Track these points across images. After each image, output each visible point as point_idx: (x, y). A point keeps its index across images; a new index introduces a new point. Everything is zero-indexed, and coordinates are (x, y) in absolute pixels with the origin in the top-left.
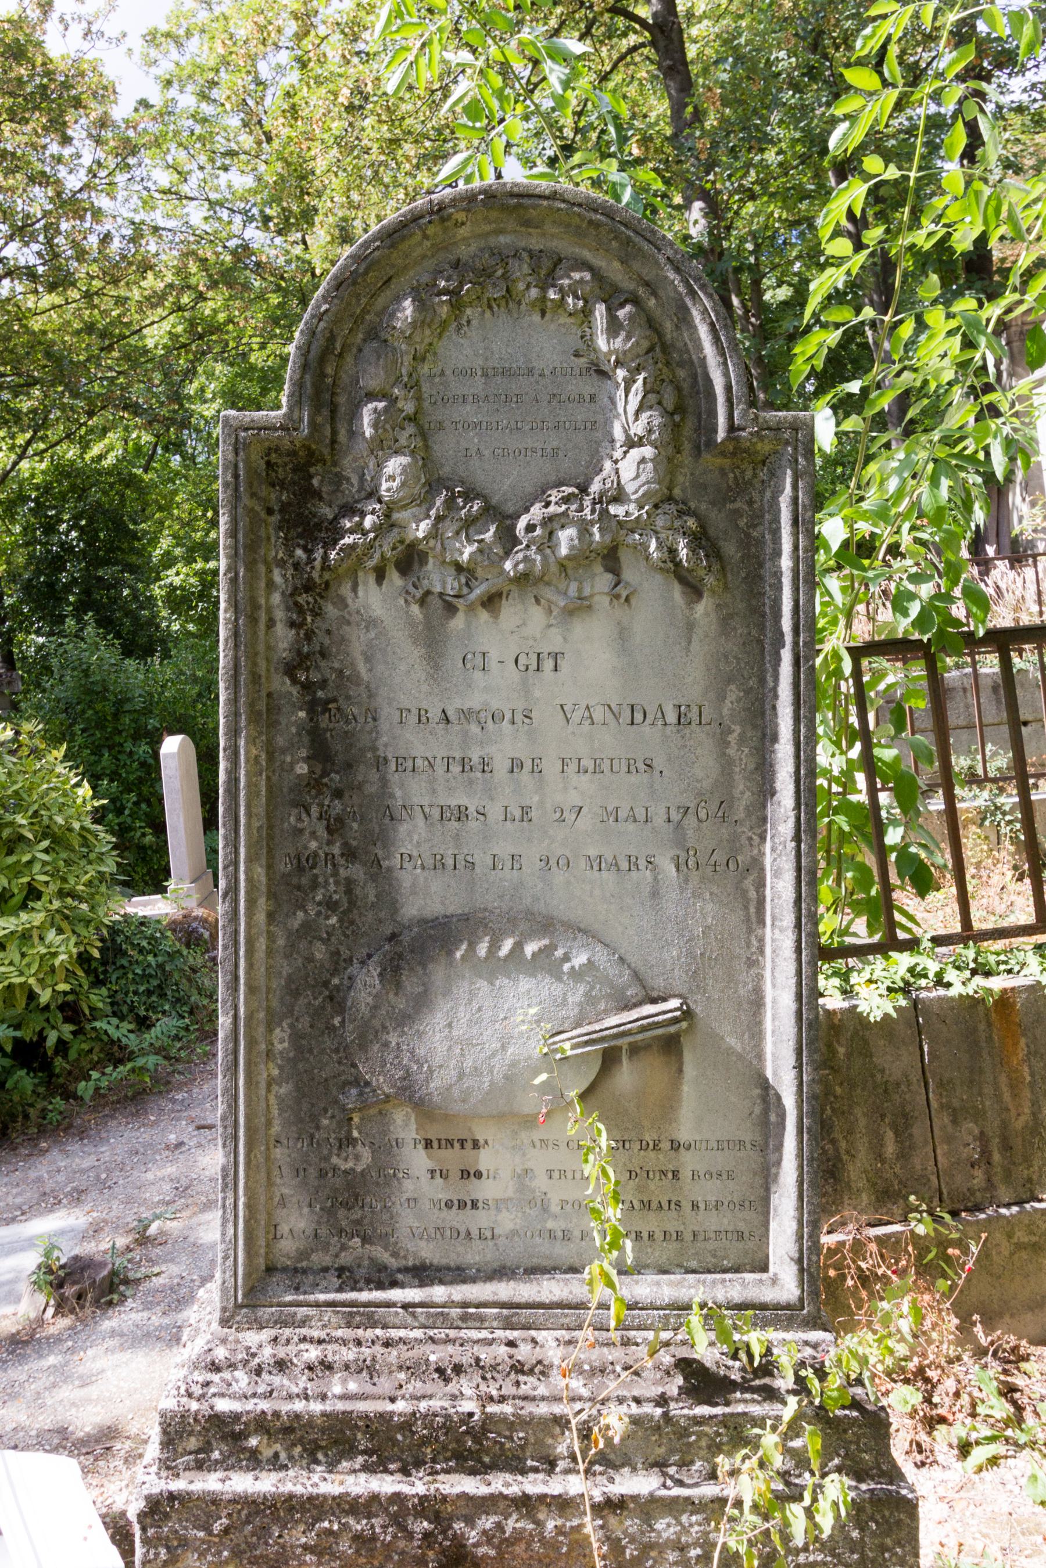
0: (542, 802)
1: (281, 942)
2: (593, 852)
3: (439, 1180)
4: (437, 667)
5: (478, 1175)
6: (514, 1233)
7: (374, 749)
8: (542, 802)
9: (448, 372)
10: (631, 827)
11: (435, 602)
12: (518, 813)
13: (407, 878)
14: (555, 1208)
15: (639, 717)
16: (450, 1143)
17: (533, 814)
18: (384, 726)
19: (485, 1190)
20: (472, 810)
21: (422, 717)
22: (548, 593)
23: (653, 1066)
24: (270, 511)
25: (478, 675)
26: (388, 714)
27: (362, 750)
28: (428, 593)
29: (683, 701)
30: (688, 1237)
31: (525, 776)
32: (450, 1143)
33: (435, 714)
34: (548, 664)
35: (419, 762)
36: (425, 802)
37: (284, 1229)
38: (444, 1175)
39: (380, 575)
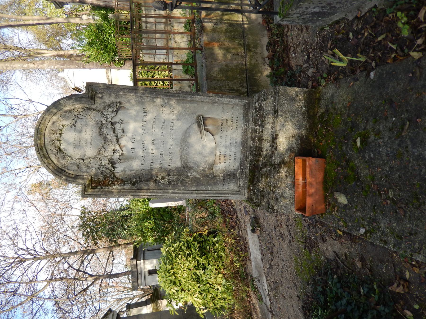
0: (161, 139)
1: (184, 188)
2: (170, 130)
3: (226, 161)
4: (134, 158)
5: (225, 154)
6: (235, 149)
7: (149, 170)
8: (161, 139)
9: (74, 153)
10: (165, 123)
11: (121, 158)
12: (162, 144)
13: (173, 166)
14: (232, 141)
15: (145, 120)
16: (220, 159)
17: (162, 141)
18: (144, 168)
19: (228, 153)
20: (161, 152)
21: (143, 161)
22: (119, 136)
23: (208, 122)
24: (102, 188)
25: (135, 150)
26: (143, 167)
27: (149, 172)
28: (119, 159)
29: (142, 112)
30: (232, 118)
31: (155, 142)
32: (220, 159)
33: (143, 158)
34: (134, 136)
35: (152, 162)
36: (159, 161)
37: (233, 188)
38: (225, 160)
39: (114, 168)
